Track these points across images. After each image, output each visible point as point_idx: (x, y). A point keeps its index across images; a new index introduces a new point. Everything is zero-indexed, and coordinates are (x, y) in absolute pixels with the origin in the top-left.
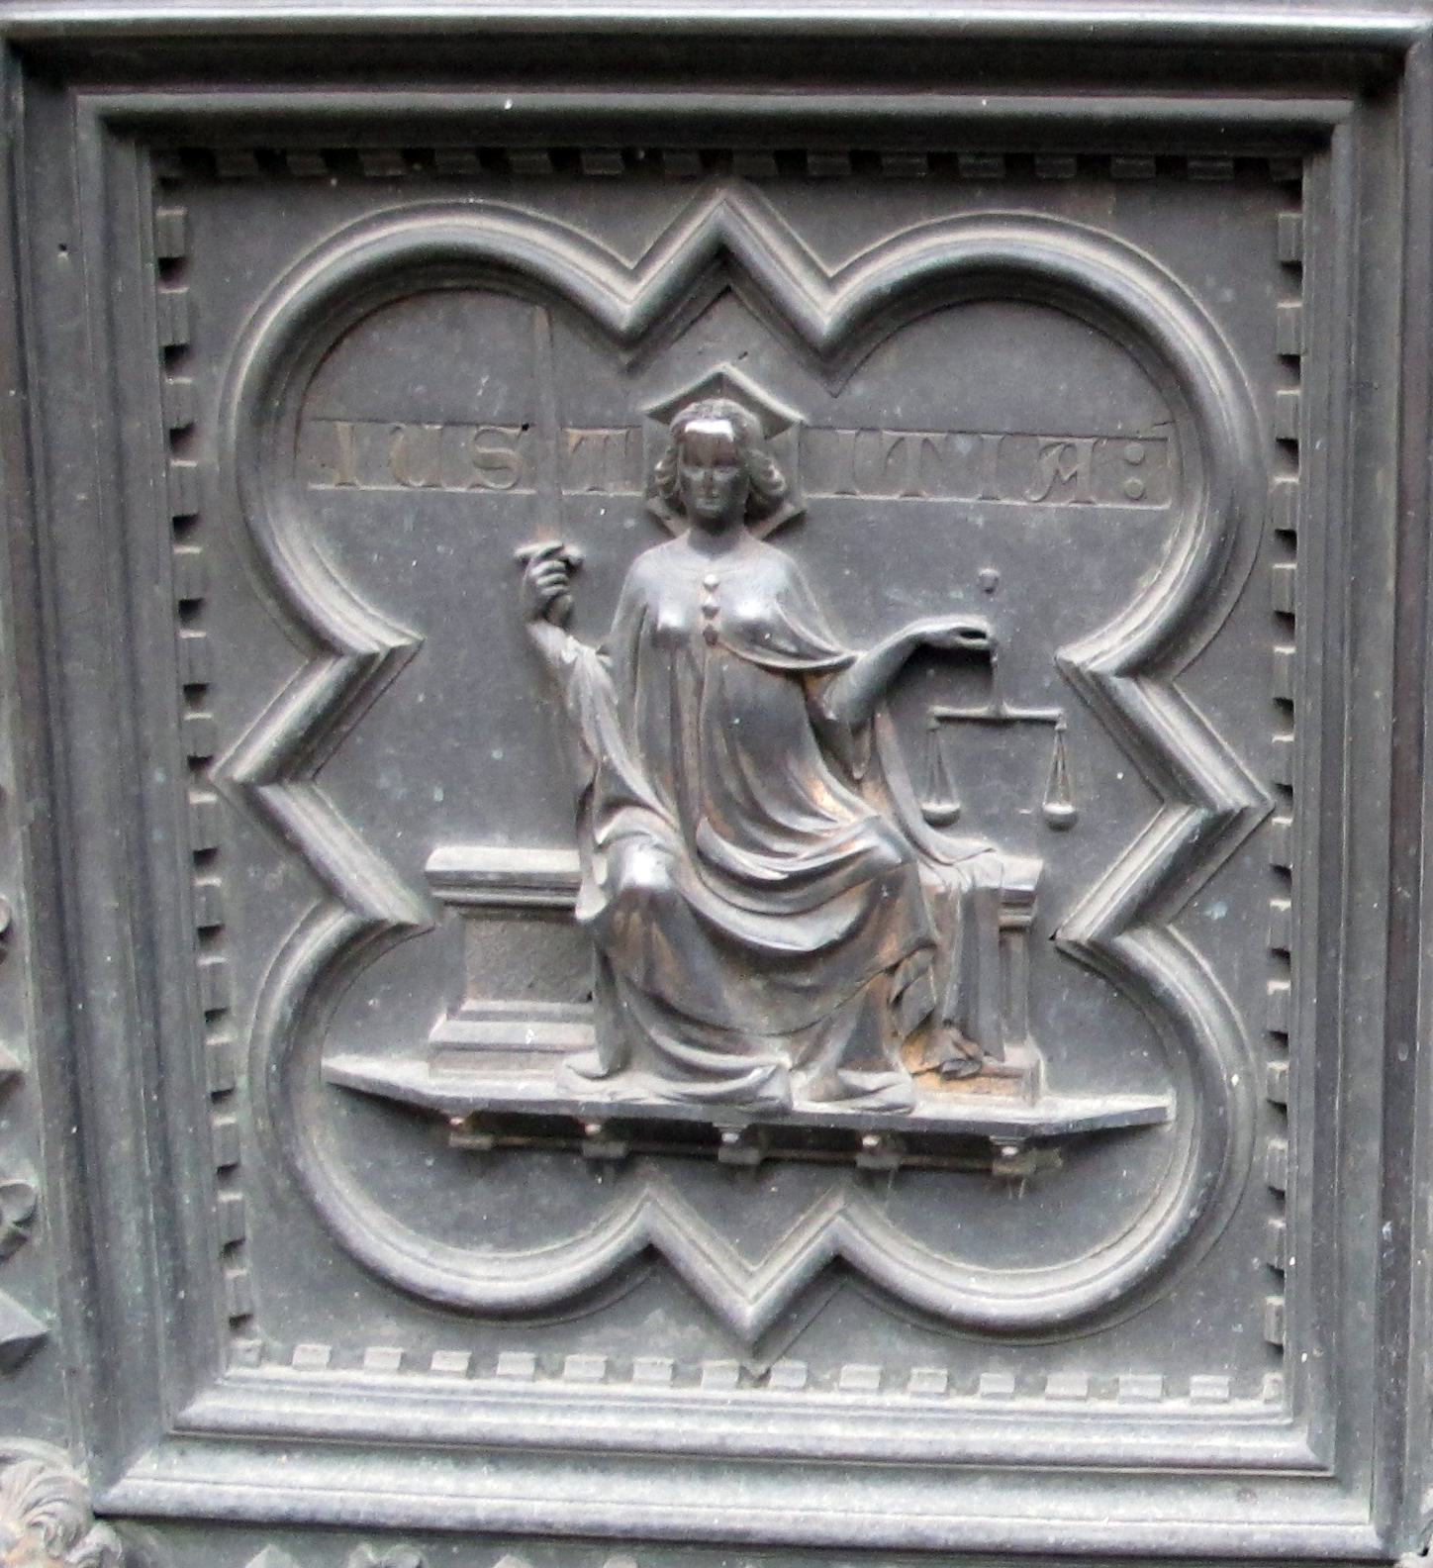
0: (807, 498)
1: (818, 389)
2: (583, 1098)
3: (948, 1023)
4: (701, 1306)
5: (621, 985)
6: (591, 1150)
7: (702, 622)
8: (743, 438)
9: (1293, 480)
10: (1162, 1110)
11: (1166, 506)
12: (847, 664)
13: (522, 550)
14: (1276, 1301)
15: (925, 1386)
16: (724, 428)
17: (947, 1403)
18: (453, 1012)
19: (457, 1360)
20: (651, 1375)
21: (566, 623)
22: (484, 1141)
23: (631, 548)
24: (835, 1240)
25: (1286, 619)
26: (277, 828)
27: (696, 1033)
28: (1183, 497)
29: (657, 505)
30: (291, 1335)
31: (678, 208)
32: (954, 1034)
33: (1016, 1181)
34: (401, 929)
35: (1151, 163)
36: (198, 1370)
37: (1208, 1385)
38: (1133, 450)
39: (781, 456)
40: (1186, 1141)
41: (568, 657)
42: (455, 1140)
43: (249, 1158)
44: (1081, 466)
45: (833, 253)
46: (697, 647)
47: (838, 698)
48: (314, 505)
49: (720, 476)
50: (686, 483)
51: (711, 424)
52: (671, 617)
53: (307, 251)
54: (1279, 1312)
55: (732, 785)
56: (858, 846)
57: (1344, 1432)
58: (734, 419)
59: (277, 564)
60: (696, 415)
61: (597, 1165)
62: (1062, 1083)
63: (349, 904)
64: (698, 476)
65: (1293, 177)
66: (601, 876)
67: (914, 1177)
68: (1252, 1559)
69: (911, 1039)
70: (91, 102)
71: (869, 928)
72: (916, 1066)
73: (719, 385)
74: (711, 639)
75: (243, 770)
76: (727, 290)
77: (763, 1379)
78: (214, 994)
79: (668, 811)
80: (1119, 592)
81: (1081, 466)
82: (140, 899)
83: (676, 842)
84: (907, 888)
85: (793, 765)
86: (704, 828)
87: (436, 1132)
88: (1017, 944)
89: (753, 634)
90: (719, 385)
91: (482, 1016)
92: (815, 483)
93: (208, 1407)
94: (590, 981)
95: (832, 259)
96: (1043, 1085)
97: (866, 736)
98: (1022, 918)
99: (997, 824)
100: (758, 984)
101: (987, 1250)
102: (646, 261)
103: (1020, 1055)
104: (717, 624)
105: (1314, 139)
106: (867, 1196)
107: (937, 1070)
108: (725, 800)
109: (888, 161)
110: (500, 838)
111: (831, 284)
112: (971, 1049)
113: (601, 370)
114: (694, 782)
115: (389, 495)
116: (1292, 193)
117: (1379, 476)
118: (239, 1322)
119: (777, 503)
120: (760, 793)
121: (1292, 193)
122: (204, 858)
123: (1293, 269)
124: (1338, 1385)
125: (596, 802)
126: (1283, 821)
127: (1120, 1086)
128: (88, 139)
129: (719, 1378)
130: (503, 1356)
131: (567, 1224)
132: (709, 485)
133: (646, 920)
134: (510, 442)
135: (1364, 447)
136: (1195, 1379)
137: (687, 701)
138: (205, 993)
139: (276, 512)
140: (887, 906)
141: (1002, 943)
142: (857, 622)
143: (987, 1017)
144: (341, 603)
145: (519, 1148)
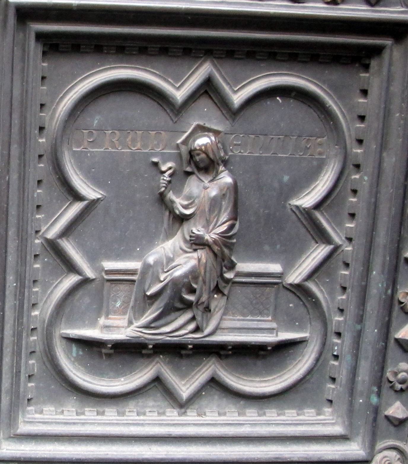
68: (220, 463)
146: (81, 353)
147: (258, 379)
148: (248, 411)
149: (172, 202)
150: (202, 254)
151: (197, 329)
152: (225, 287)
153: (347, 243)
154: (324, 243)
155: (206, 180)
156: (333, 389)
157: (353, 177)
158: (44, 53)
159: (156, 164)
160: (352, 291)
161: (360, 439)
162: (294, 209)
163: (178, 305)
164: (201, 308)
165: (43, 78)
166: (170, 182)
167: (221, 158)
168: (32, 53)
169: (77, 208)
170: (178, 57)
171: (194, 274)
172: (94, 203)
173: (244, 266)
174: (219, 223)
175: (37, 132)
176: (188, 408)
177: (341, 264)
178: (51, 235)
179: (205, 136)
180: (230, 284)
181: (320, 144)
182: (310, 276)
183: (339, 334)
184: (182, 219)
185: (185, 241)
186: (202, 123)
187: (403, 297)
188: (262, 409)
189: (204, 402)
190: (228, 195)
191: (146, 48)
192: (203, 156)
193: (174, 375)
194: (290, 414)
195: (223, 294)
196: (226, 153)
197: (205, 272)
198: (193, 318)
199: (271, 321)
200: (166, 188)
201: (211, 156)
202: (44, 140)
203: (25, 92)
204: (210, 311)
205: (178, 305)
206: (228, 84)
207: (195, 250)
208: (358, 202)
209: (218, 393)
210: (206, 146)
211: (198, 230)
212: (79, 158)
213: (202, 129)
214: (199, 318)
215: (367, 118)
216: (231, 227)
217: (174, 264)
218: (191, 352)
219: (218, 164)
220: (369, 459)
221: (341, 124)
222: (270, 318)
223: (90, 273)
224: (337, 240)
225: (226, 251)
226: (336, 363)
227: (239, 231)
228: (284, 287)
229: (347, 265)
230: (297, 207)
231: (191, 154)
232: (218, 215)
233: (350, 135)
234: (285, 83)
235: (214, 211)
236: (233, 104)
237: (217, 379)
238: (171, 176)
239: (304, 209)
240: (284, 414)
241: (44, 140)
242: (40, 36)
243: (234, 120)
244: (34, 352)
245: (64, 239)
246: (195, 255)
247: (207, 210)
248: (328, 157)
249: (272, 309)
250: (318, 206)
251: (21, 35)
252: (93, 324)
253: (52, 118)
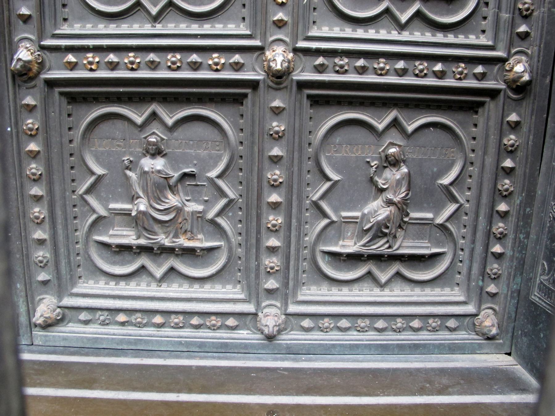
0: (167, 151)
1: (169, 134)
2: (133, 243)
3: (189, 231)
4: (151, 275)
5: (139, 226)
6: (134, 251)
7: (151, 170)
8: (157, 141)
9: (242, 148)
10: (222, 245)
11: (222, 152)
12: (173, 176)
13: (123, 159)
14: (239, 274)
15: (185, 287)
16: (154, 140)
17: (189, 290)
18: (113, 230)
19: (114, 283)
20: (143, 285)
21: (130, 170)
22: (118, 250)
23: (140, 158)
24: (172, 265)
25: (241, 169)
26: (86, 201)
27: (150, 233)
28: (225, 151)
29: (144, 152)
30: (88, 279)
31: (147, 106)
32: (190, 233)
33: (199, 256)
34: (105, 217)
35: (220, 99)
36: (74, 285)
37: (229, 287)
38: (217, 143)
39: (163, 144)
40: (225, 249)
41: (131, 175)
42: (113, 249)
43: (81, 252)
44: (209, 146)
45: (171, 113)
46: (150, 174)
47: (172, 181)
48: (91, 152)
49: (154, 147)
50: (149, 148)
51: (153, 139)
52: (146, 169)
53: (90, 113)
54: (240, 276)
55: (156, 195)
56: (175, 204)
57: (250, 294)
58: (156, 139)
59: (86, 161)
60: (150, 138)
61: (135, 253)
62: (207, 241)
63: (97, 213)
64: (150, 147)
65: (242, 101)
66: (136, 209)
67: (184, 255)
69: (183, 234)
70: (57, 90)
71: (177, 217)
72: (184, 238)
73: (154, 133)
74: (153, 172)
75: (80, 193)
76: (155, 119)
77: (160, 286)
78: (76, 227)
79: (146, 199)
80: (215, 165)
81: (209, 146)
82: (65, 212)
83: (147, 204)
84: (182, 211)
85: (165, 192)
86: (151, 201)
87: (110, 248)
88: (199, 219)
89: (159, 172)
90: (154, 133)
91: (117, 230)
92: (169, 148)
93: (75, 290)
94: (134, 225)
95: (171, 114)
96: (204, 241)
97: (176, 187)
98: (200, 215)
99: (197, 201)
100: (160, 225)
101: (195, 266)
102: (143, 114)
103: (200, 236)
104: (153, 170)
105: (245, 96)
106: (176, 258)
107: (187, 239)
108: (155, 197)
109: (180, 99)
110: (120, 203)
111: (171, 118)
112: (193, 235)
113: (136, 131)
114: (150, 194)
115: (103, 150)
116: (242, 104)
117: (255, 147)
118: (80, 277)
119: (163, 151)
120: (160, 196)
121: (242, 104)
122: (74, 206)
123: (242, 115)
124: (249, 287)
125: (135, 197)
126: (240, 200)
127: (215, 241)
128: (57, 96)
129: (154, 286)
130: (121, 282)
131: (130, 262)
132: (152, 148)
133: (143, 216)
134: (122, 142)
135: (253, 143)
136: (227, 286)
137: (149, 182)
138: (75, 227)
139: (86, 153)
140: (180, 213)
141: (197, 219)
142: (175, 170)
143: (195, 230)
144: (96, 167)
145: (123, 251)
146: (330, 259)
147: (421, 273)
148: (415, 289)
149: (377, 182)
150: (392, 208)
151: (390, 247)
152: (404, 225)
153: (466, 202)
154: (455, 203)
155: (394, 170)
156: (460, 278)
157: (470, 169)
158: (311, 105)
159: (368, 162)
160: (469, 227)
161: (473, 303)
162: (439, 185)
163: (380, 235)
164: (392, 236)
165: (311, 118)
166: (375, 171)
167: (402, 159)
168: (305, 105)
169: (328, 185)
170: (380, 107)
171: (388, 219)
172: (337, 182)
173: (415, 215)
174: (401, 192)
175: (307, 145)
176: (385, 288)
177: (463, 213)
178: (314, 199)
179: (394, 148)
180: (407, 223)
181: (453, 152)
182: (448, 220)
183: (462, 250)
184: (382, 190)
185: (383, 201)
186: (392, 141)
187: (495, 230)
188: (423, 288)
189: (393, 284)
190: (405, 178)
191: (363, 103)
192: (393, 158)
193: (378, 270)
194: (437, 291)
195: (403, 229)
196: (404, 156)
197: (394, 218)
198: (388, 242)
199: (427, 243)
200: (374, 174)
201: (397, 158)
202: (311, 150)
203: (301, 125)
204: (396, 238)
205: (380, 235)
206: (405, 121)
207: (389, 206)
208: (472, 182)
209: (400, 280)
210: (394, 153)
211: (390, 196)
212: (329, 159)
213: (392, 144)
214: (390, 241)
215: (477, 138)
216: (407, 195)
217: (378, 213)
218: (386, 259)
219: (401, 162)
220: (478, 314)
221: (463, 141)
222: (427, 241)
223: (334, 218)
224: (462, 201)
225: (404, 207)
226: (461, 264)
227: (411, 196)
228: (434, 225)
229: (466, 214)
230: (441, 184)
231: (387, 157)
232: (401, 189)
233: (468, 147)
234: (435, 121)
235: (398, 186)
236: (408, 131)
237: (400, 272)
238: (376, 168)
239: (445, 185)
240: (434, 291)
241: (311, 150)
242: (309, 97)
243: (408, 140)
244: (306, 259)
245: (321, 201)
246: (389, 209)
247: (395, 186)
248: (457, 159)
249: (428, 236)
250: (452, 184)
251: (299, 96)
252: (336, 244)
253: (315, 138)
